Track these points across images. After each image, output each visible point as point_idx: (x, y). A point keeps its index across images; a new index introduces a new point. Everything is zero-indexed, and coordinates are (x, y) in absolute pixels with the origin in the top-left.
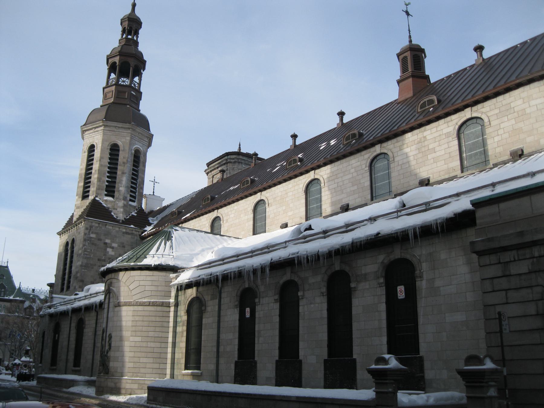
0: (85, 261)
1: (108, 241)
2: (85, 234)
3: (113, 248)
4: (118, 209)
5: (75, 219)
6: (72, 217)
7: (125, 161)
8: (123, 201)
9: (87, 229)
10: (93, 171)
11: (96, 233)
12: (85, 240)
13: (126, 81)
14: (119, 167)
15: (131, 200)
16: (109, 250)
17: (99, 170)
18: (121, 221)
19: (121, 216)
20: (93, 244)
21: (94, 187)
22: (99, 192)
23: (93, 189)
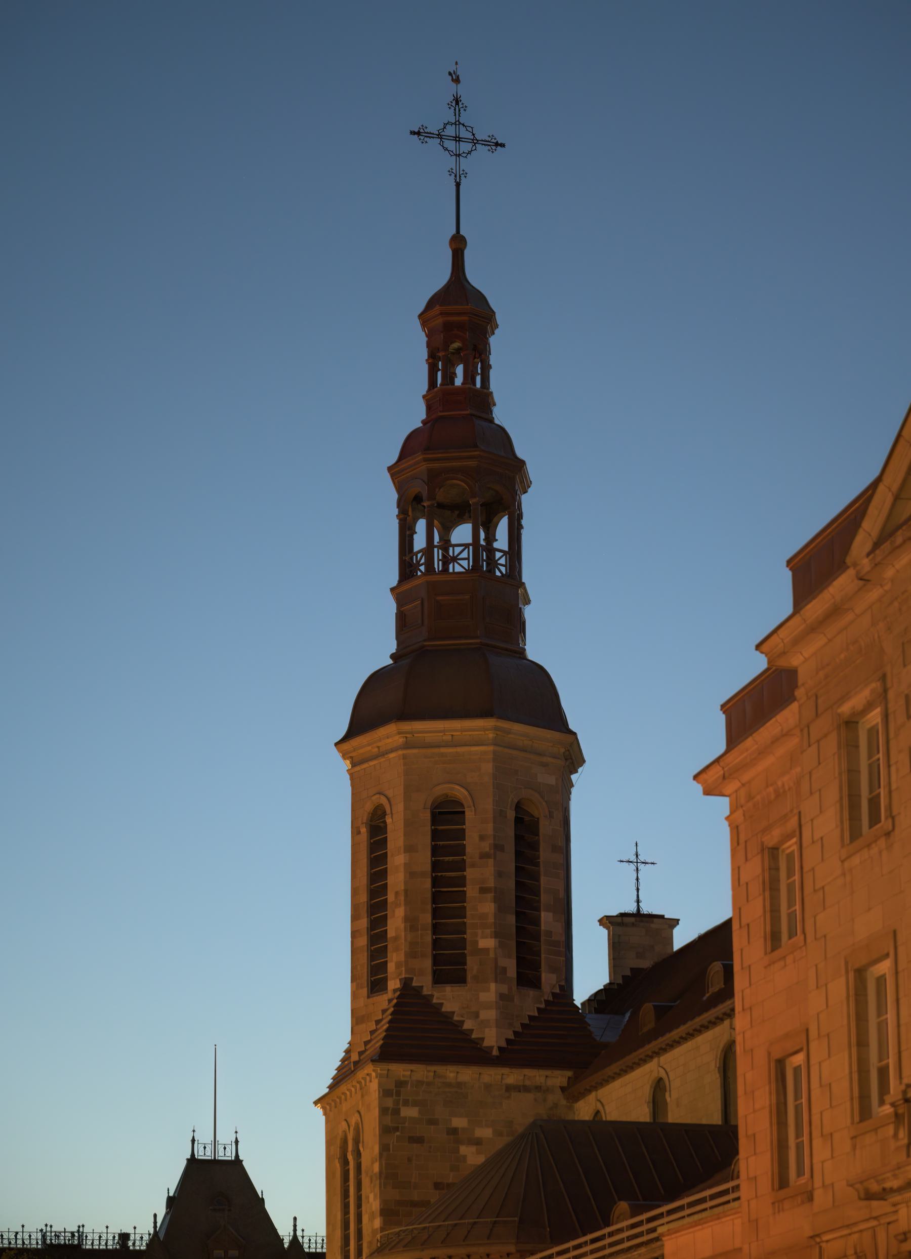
1: (459, 1122)
2: (383, 1111)
3: (478, 1142)
4: (485, 1015)
7: (486, 846)
8: (493, 986)
10: (391, 897)
11: (415, 1104)
12: (385, 1130)
13: (460, 557)
14: (469, 873)
16: (464, 1150)
17: (406, 891)
18: (495, 1052)
23: (395, 961)
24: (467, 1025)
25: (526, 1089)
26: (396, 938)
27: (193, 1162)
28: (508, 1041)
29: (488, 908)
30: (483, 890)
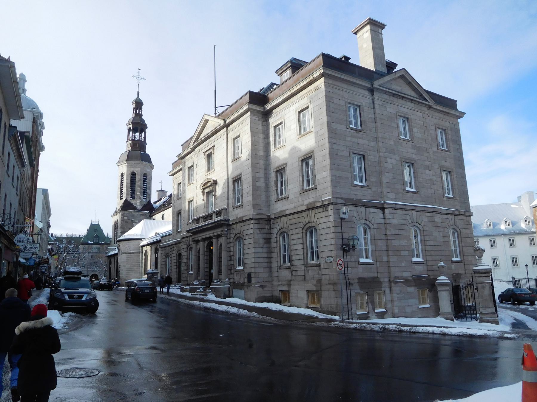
0: (123, 230)
1: (133, 220)
2: (121, 218)
4: (138, 204)
5: (117, 210)
6: (116, 210)
8: (139, 200)
9: (122, 215)
11: (126, 217)
15: (143, 198)
19: (139, 207)
20: (126, 222)
21: (125, 194)
22: (127, 196)
24: (135, 206)
25: (144, 215)
26: (125, 192)
27: (91, 224)
28: (141, 208)
29: (139, 189)
30: (138, 186)
